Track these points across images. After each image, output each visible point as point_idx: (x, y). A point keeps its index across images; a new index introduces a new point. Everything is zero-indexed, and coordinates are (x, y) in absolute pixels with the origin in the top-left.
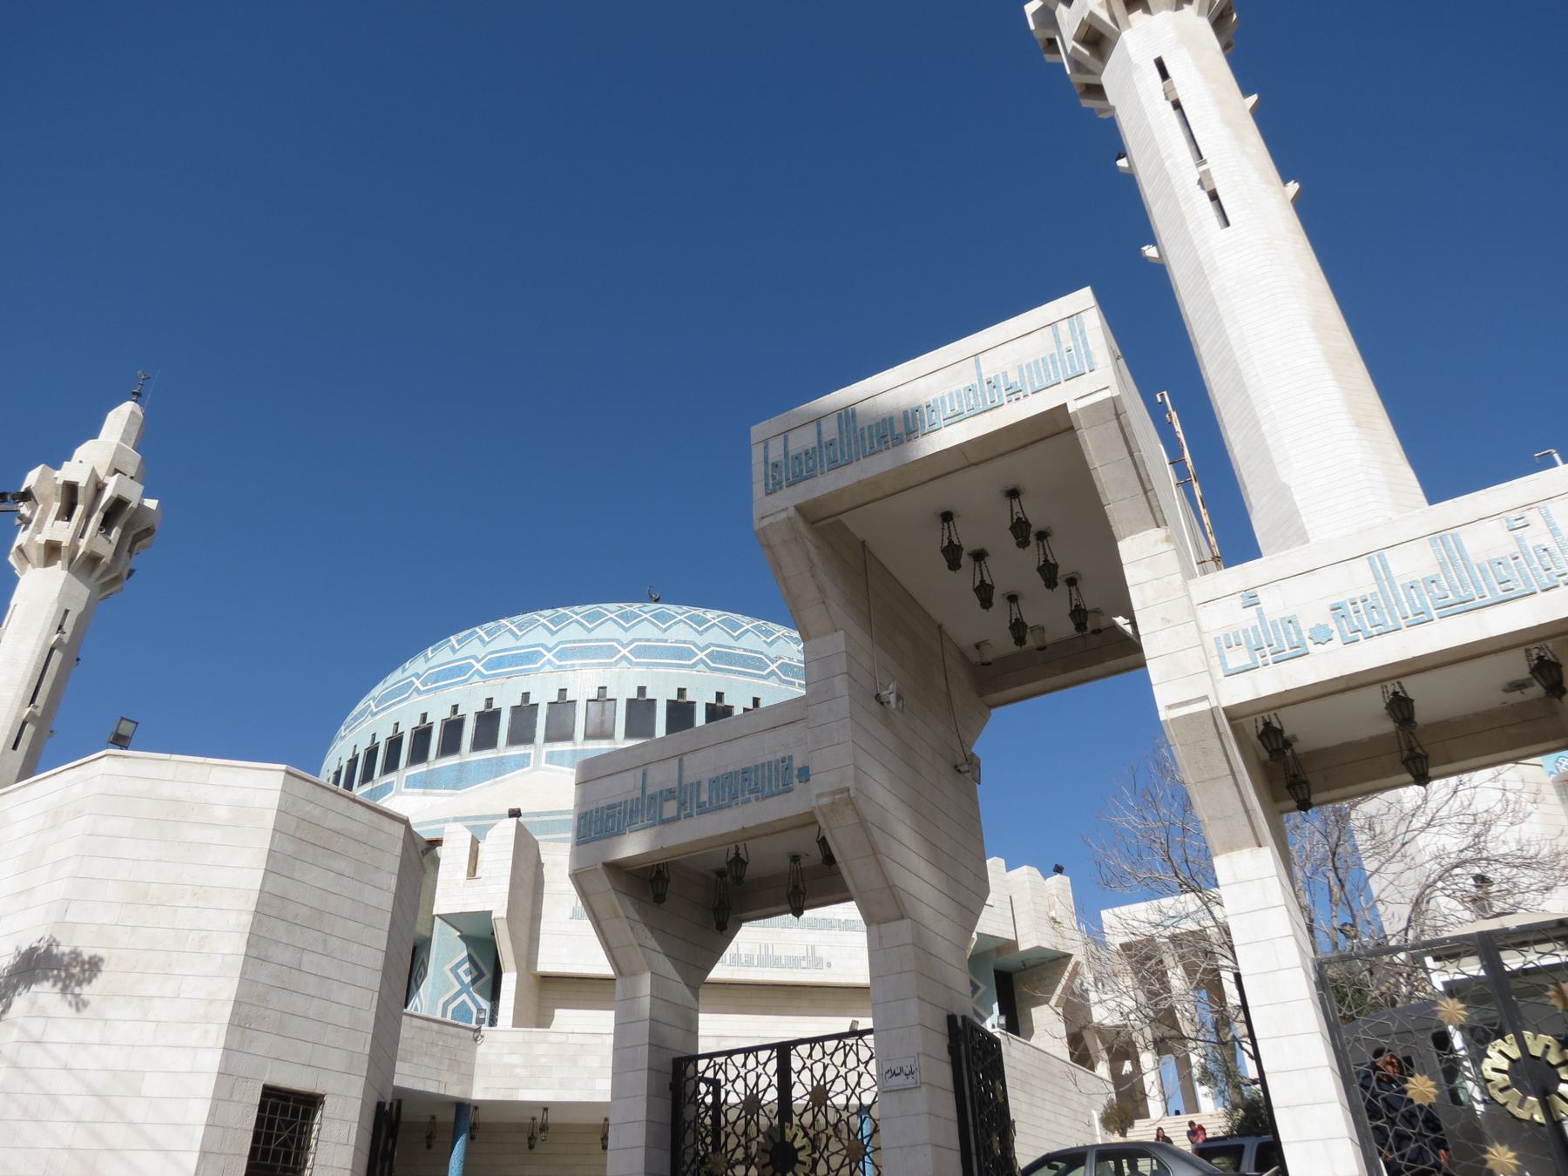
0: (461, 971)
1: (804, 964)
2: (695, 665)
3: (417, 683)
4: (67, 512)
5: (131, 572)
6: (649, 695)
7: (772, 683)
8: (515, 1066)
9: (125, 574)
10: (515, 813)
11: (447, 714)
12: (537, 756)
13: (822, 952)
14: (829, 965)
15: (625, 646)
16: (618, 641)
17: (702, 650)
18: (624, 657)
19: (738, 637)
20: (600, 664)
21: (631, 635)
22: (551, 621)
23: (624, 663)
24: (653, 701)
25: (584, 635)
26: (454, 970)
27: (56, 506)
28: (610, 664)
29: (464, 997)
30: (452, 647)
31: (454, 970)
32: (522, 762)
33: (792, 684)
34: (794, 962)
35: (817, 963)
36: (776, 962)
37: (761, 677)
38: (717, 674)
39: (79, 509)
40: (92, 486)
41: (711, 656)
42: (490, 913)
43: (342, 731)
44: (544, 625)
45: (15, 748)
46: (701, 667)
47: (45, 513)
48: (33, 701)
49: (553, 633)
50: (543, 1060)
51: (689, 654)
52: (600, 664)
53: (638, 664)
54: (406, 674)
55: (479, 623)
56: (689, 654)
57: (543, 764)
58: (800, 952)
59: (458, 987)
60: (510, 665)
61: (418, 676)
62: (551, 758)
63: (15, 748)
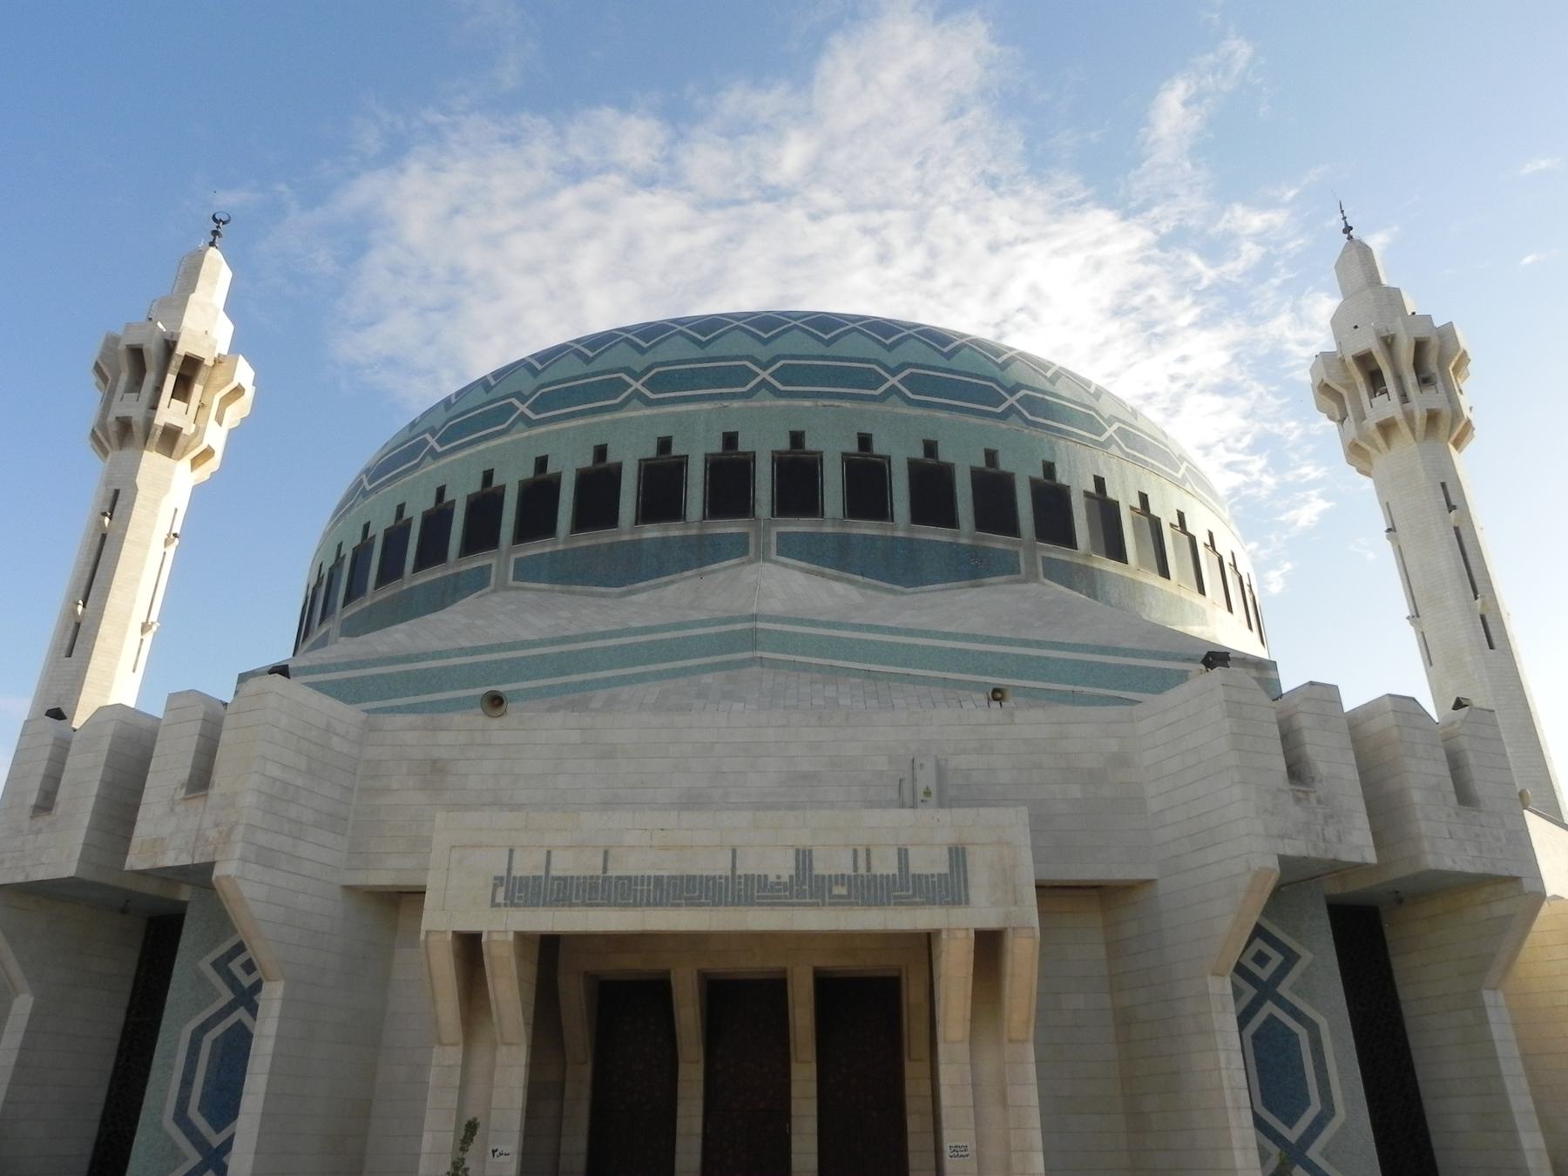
16: (628, 371)
21: (649, 358)
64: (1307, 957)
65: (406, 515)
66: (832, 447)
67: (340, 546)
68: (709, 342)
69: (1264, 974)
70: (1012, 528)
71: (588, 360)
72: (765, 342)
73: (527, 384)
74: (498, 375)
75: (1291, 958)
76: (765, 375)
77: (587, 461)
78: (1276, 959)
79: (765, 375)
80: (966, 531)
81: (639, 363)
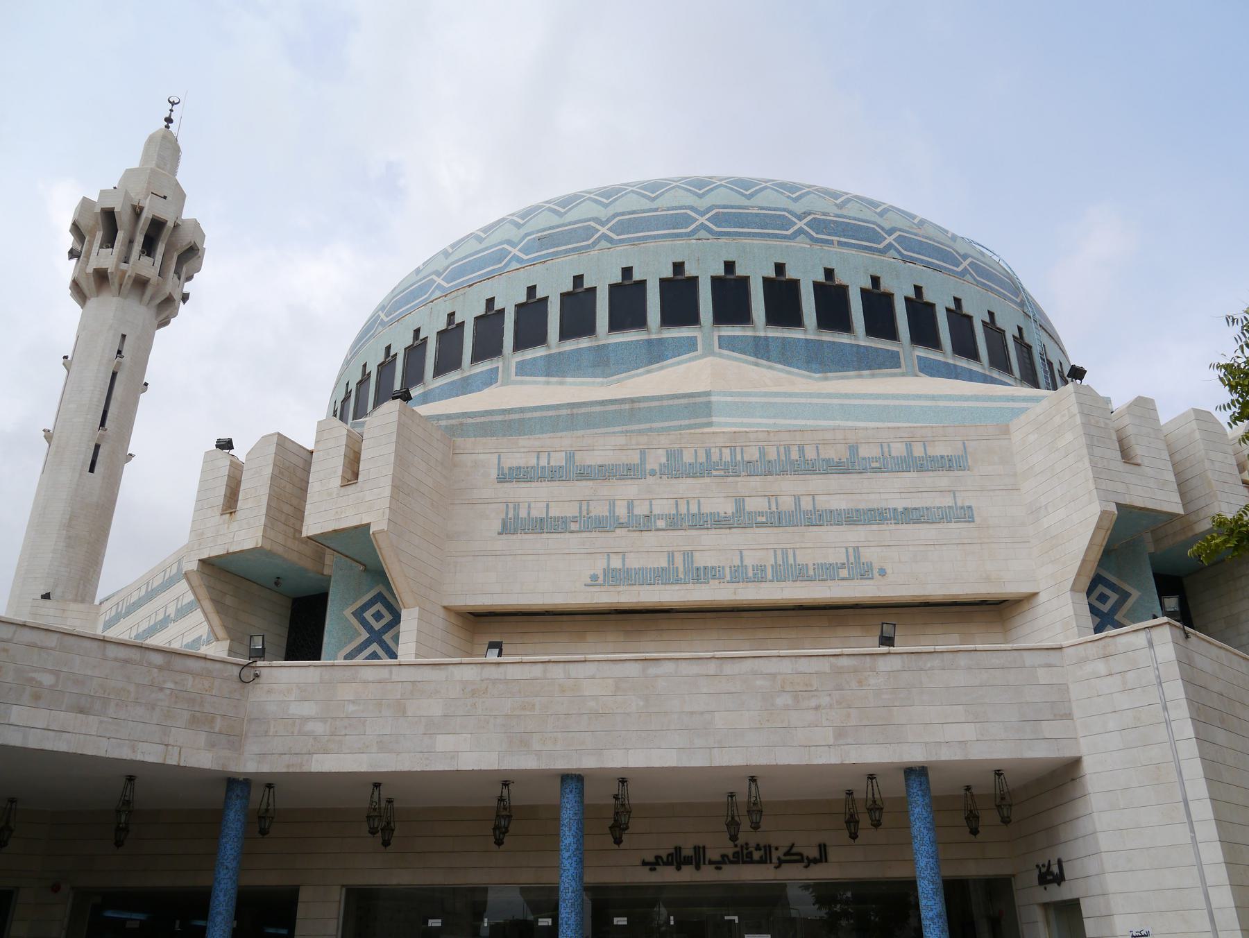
1: (844, 573)
4: (109, 241)
6: (637, 276)
7: (801, 244)
8: (306, 719)
11: (409, 340)
12: (506, 369)
13: (869, 555)
14: (883, 573)
16: (596, 220)
18: (604, 236)
19: (752, 195)
21: (611, 211)
24: (643, 282)
27: (99, 235)
28: (588, 247)
31: (359, 614)
33: (830, 242)
34: (828, 572)
35: (865, 572)
36: (801, 574)
37: (785, 237)
38: (723, 241)
39: (120, 236)
40: (129, 210)
45: (92, 470)
46: (703, 234)
47: (91, 244)
48: (103, 424)
50: (351, 708)
52: (574, 250)
53: (621, 241)
56: (688, 220)
57: (513, 377)
58: (836, 557)
59: (365, 635)
62: (523, 369)
63: (92, 470)
64: (1135, 594)
66: (756, 270)
68: (656, 198)
69: (1105, 608)
70: (892, 335)
71: (560, 215)
72: (700, 196)
73: (514, 234)
74: (485, 230)
75: (1125, 596)
78: (1114, 597)
79: (702, 220)
80: (859, 336)
81: (603, 213)
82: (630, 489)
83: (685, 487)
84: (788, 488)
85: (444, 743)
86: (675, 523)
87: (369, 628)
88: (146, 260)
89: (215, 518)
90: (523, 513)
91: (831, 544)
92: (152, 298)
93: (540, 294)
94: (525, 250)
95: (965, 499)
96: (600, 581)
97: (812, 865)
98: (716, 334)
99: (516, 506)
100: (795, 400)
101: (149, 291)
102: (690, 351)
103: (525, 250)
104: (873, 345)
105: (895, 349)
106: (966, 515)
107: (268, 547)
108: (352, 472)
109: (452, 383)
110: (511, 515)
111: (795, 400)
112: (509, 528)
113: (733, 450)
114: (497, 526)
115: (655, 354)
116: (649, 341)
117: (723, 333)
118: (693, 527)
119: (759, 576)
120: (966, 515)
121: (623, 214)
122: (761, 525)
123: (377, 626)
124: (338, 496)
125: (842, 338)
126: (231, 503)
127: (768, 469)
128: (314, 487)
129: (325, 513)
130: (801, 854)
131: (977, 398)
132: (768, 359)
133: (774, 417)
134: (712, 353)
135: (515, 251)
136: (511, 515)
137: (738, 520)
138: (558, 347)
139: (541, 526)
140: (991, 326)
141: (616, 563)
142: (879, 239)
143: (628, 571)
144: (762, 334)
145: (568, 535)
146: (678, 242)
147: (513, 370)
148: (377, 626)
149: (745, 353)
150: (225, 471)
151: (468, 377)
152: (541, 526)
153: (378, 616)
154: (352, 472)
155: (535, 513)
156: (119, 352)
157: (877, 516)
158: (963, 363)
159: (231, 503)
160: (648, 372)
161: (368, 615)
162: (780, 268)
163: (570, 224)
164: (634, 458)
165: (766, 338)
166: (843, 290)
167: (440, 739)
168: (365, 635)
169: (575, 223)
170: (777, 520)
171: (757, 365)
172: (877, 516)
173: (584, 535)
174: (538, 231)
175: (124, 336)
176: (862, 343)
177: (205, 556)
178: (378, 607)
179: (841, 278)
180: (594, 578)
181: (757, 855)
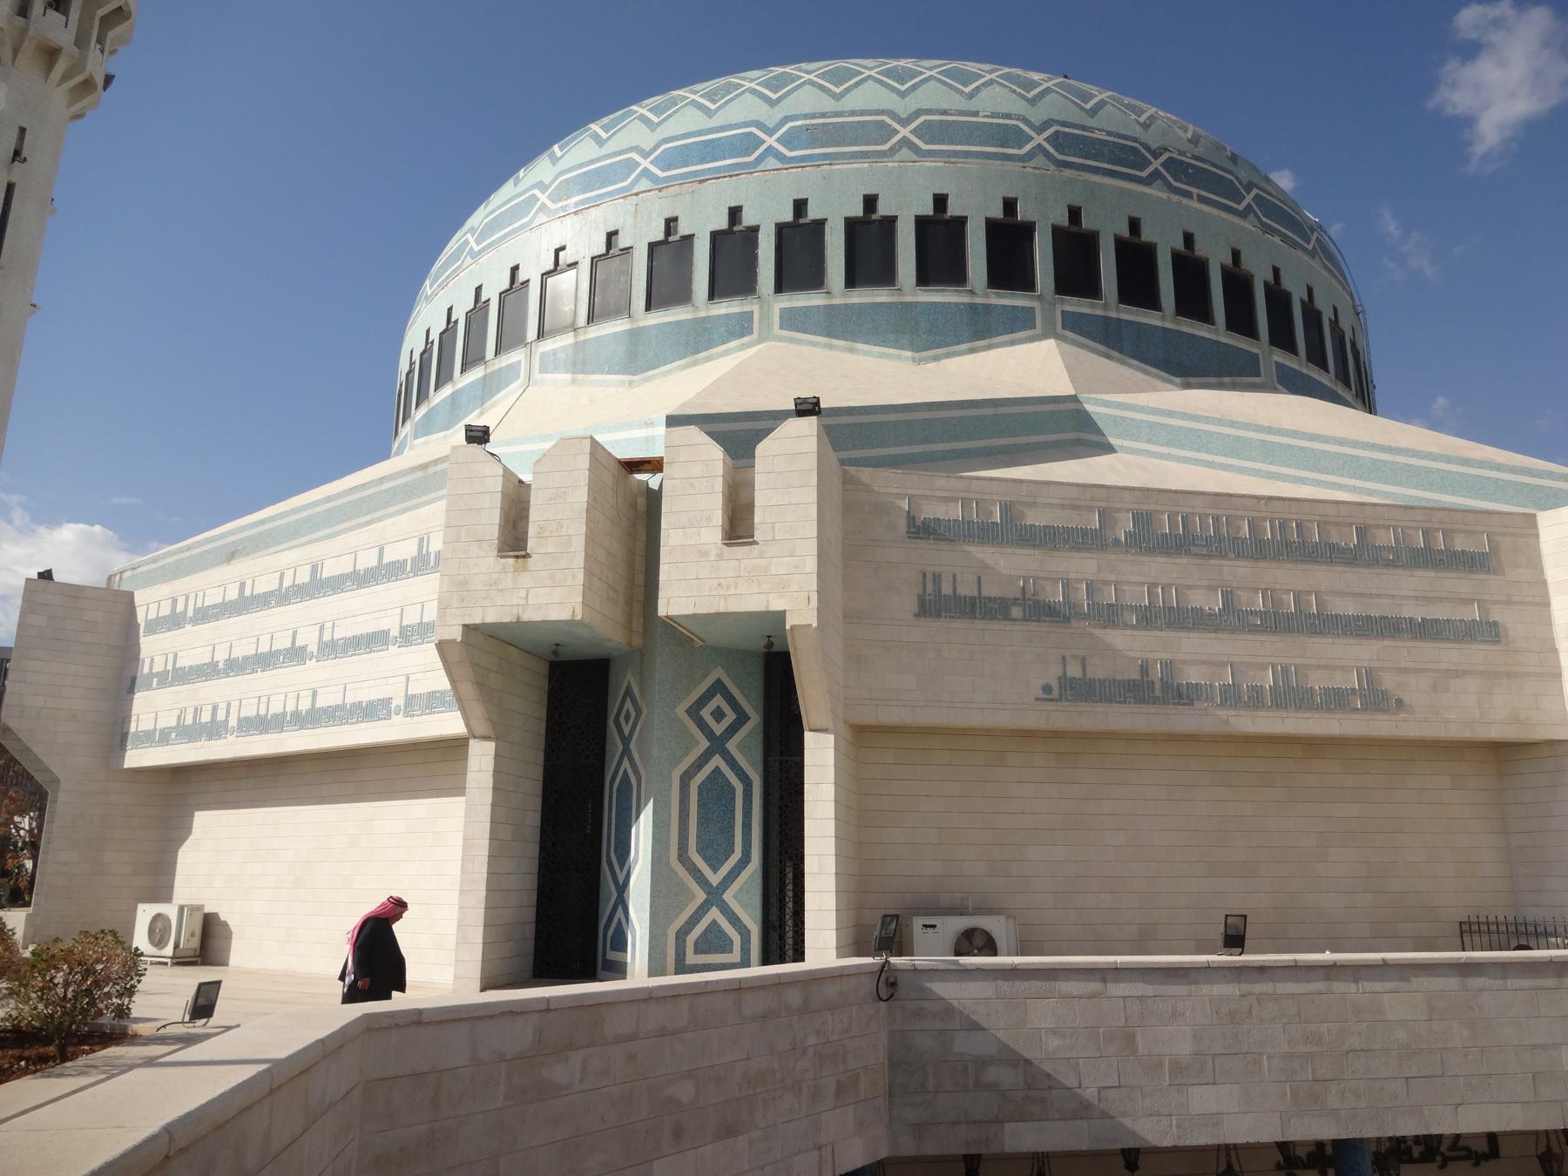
0: (706, 713)
2: (1029, 156)
3: (543, 198)
5: (109, 79)
9: (100, 80)
10: (807, 408)
12: (765, 316)
13: (1388, 682)
15: (904, 122)
17: (1040, 130)
20: (864, 155)
22: (765, 84)
23: (905, 153)
25: (828, 104)
26: (694, 712)
29: (717, 761)
30: (596, 137)
32: (741, 327)
33: (1188, 195)
34: (1336, 700)
35: (1376, 699)
37: (1139, 180)
38: (1067, 173)
41: (1054, 139)
42: (781, 616)
43: (427, 287)
44: (753, 91)
49: (772, 103)
51: (1020, 138)
52: (864, 155)
53: (931, 153)
54: (521, 187)
55: (637, 99)
57: (776, 330)
59: (704, 744)
60: (703, 161)
61: (542, 186)
65: (522, 277)
67: (450, 310)
76: (904, 132)
77: (722, 223)
82: (1083, 566)
83: (1161, 569)
84: (1289, 579)
85: (1202, 1098)
86: (1147, 618)
87: (709, 733)
88: (53, 15)
89: (486, 562)
90: (946, 589)
91: (1339, 661)
92: (65, 77)
93: (813, 213)
94: (787, 140)
95: (1496, 615)
96: (1056, 694)
97: (1483, 1163)
98: (1059, 308)
99: (937, 578)
100: (1195, 425)
101: (61, 66)
102: (1025, 328)
103: (787, 140)
104: (1232, 343)
105: (1255, 350)
106: (1490, 632)
107: (587, 621)
108: (738, 524)
109: (678, 323)
110: (929, 589)
111: (1195, 425)
112: (933, 606)
113: (1217, 519)
114: (912, 605)
115: (981, 328)
116: (973, 307)
117: (1068, 308)
118: (1170, 625)
119: (1255, 699)
120: (1490, 632)
121: (929, 112)
122: (1254, 629)
123: (719, 729)
124: (720, 557)
125: (1201, 331)
126: (514, 538)
127: (1258, 550)
128: (671, 537)
129: (700, 580)
130: (1468, 1149)
131: (1480, 464)
132: (1121, 351)
133: (1167, 444)
134: (1058, 337)
135: (771, 141)
136: (929, 589)
137: (1231, 619)
138: (844, 295)
139: (978, 608)
140: (1312, 317)
141: (1074, 671)
142: (1239, 198)
143: (1091, 682)
144: (1113, 314)
145: (1008, 626)
146: (1009, 165)
147: (776, 319)
148: (719, 729)
149: (1093, 339)
150: (497, 485)
151: (704, 319)
152: (978, 608)
153: (718, 715)
154: (738, 524)
155: (963, 591)
156: (17, 153)
157: (1389, 628)
158: (1315, 373)
159: (514, 538)
160: (973, 351)
161: (706, 713)
162: (1134, 225)
163: (853, 113)
164: (1095, 522)
165: (1119, 320)
166: (1149, 251)
167: (1196, 1092)
168: (704, 744)
169: (863, 113)
170: (1276, 623)
171: (1108, 357)
172: (1389, 628)
173: (1033, 626)
174: (806, 117)
175: (23, 130)
176: (1223, 340)
177: (476, 619)
178: (718, 701)
179: (1201, 249)
180: (1047, 689)
181: (1417, 1151)
